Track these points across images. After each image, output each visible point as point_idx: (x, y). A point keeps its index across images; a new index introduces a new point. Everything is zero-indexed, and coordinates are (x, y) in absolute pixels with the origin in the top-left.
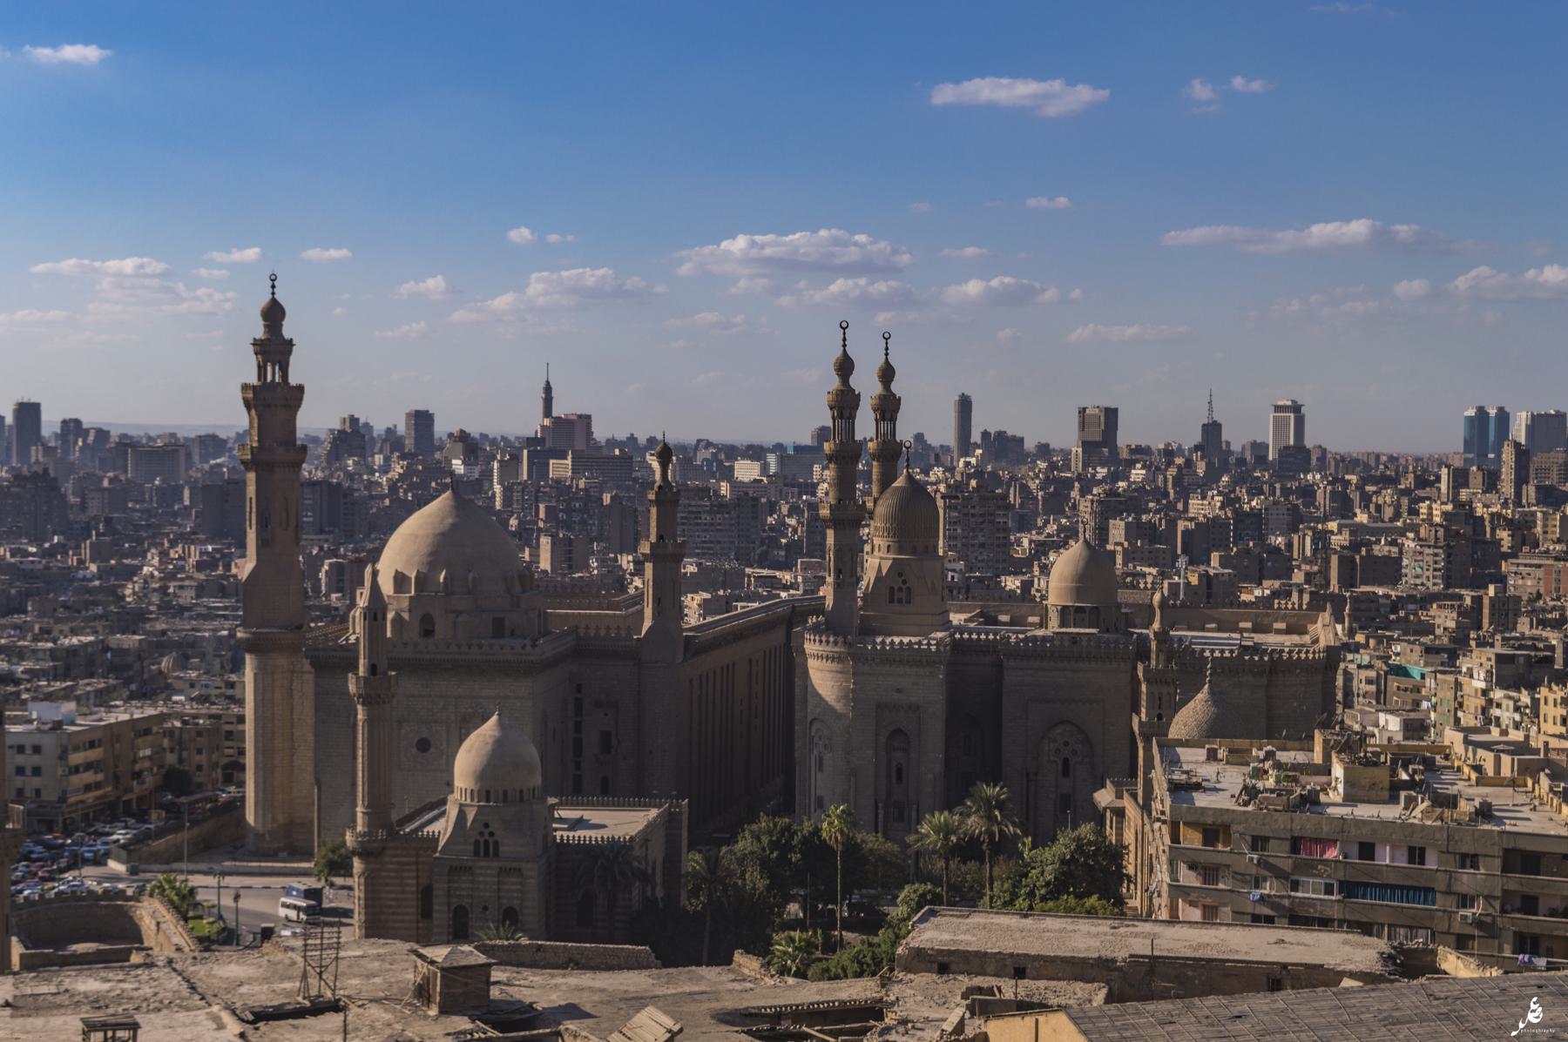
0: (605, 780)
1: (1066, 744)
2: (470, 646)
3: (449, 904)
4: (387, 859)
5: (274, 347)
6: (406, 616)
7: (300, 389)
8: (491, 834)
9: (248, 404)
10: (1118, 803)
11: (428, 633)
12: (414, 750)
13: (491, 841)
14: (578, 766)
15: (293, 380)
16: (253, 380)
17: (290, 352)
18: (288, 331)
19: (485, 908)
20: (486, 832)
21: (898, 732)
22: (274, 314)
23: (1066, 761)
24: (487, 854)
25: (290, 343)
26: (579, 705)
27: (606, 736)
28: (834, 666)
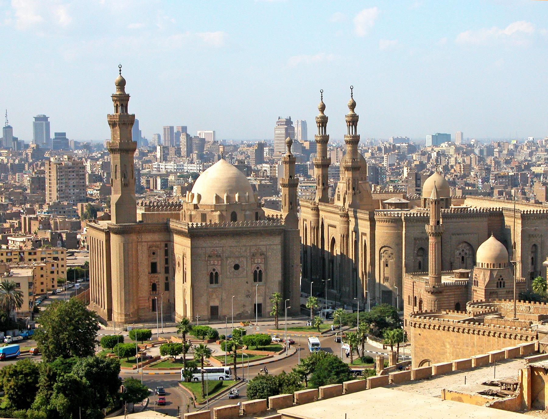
1: (463, 251)
4: (444, 294)
5: (122, 100)
6: (224, 213)
7: (133, 116)
8: (502, 279)
13: (502, 282)
15: (130, 112)
18: (127, 91)
22: (121, 84)
23: (463, 257)
24: (500, 287)
25: (128, 96)
28: (393, 224)
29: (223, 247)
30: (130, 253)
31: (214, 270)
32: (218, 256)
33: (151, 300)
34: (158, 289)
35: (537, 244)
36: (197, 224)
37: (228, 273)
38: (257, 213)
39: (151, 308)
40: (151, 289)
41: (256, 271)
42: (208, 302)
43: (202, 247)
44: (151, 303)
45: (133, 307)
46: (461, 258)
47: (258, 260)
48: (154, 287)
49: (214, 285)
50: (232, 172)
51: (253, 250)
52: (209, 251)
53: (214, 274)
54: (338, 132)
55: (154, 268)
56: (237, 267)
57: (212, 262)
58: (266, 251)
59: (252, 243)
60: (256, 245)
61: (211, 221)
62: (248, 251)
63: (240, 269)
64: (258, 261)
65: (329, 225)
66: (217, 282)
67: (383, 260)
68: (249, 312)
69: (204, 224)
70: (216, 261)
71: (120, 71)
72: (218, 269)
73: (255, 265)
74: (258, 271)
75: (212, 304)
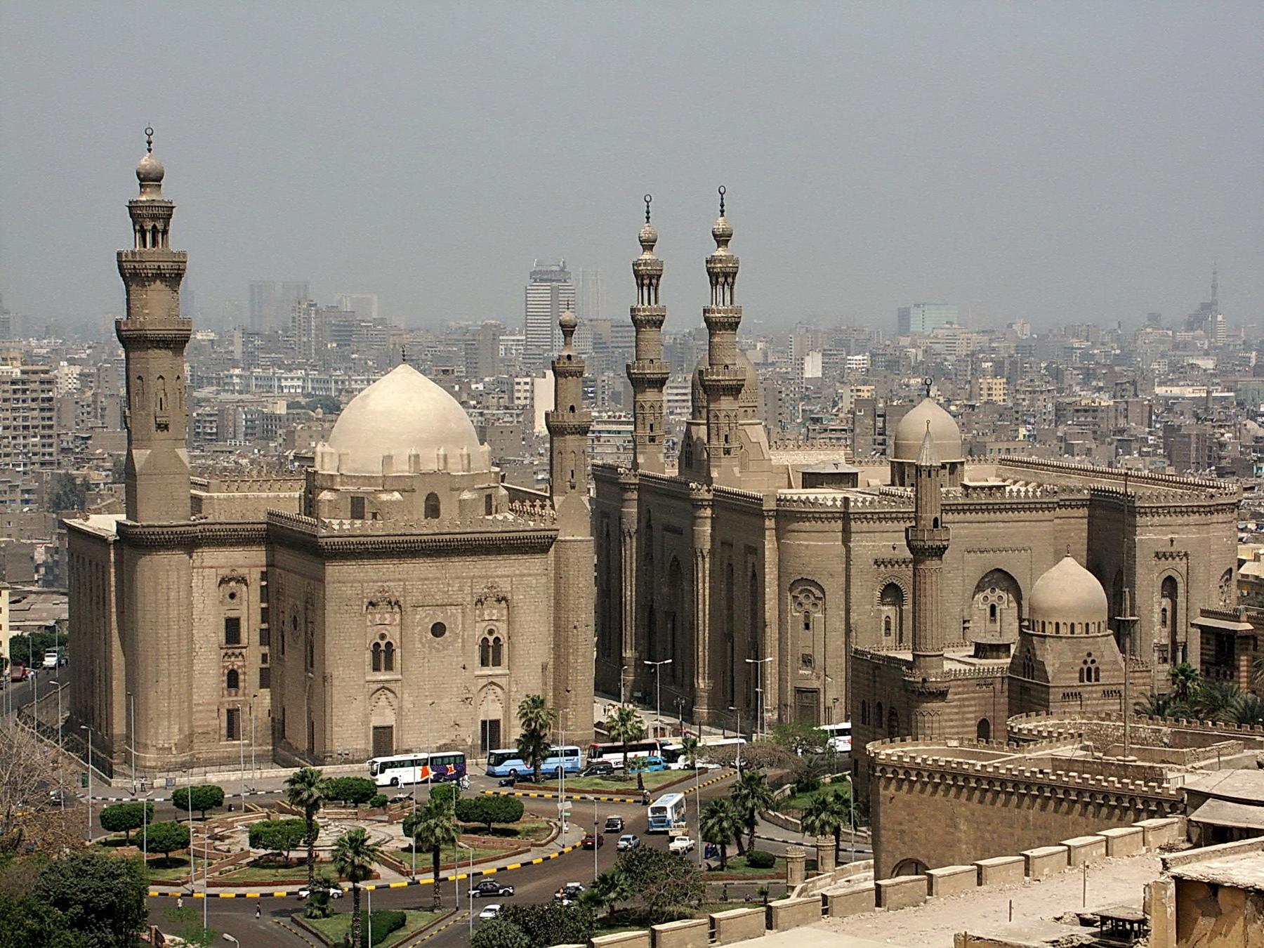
12: (430, 635)
13: (1093, 667)
20: (1089, 660)
23: (993, 608)
24: (1089, 679)
29: (404, 580)
30: (173, 594)
31: (383, 637)
32: (394, 604)
33: (224, 711)
34: (241, 684)
35: (1174, 575)
36: (341, 524)
37: (418, 645)
38: (489, 497)
39: (224, 732)
40: (225, 685)
41: (485, 640)
42: (367, 717)
43: (352, 582)
44: (225, 718)
45: (180, 730)
47: (494, 612)
48: (233, 679)
49: (382, 676)
51: (480, 589)
52: (371, 591)
53: (383, 648)
54: (685, 299)
55: (232, 628)
56: (438, 630)
57: (378, 616)
58: (511, 592)
59: (476, 572)
60: (487, 577)
61: (374, 516)
62: (467, 589)
63: (447, 634)
64: (491, 614)
65: (667, 528)
66: (389, 667)
68: (469, 741)
69: (358, 523)
70: (387, 616)
72: (394, 635)
73: (484, 624)
74: (491, 639)
75: (377, 721)
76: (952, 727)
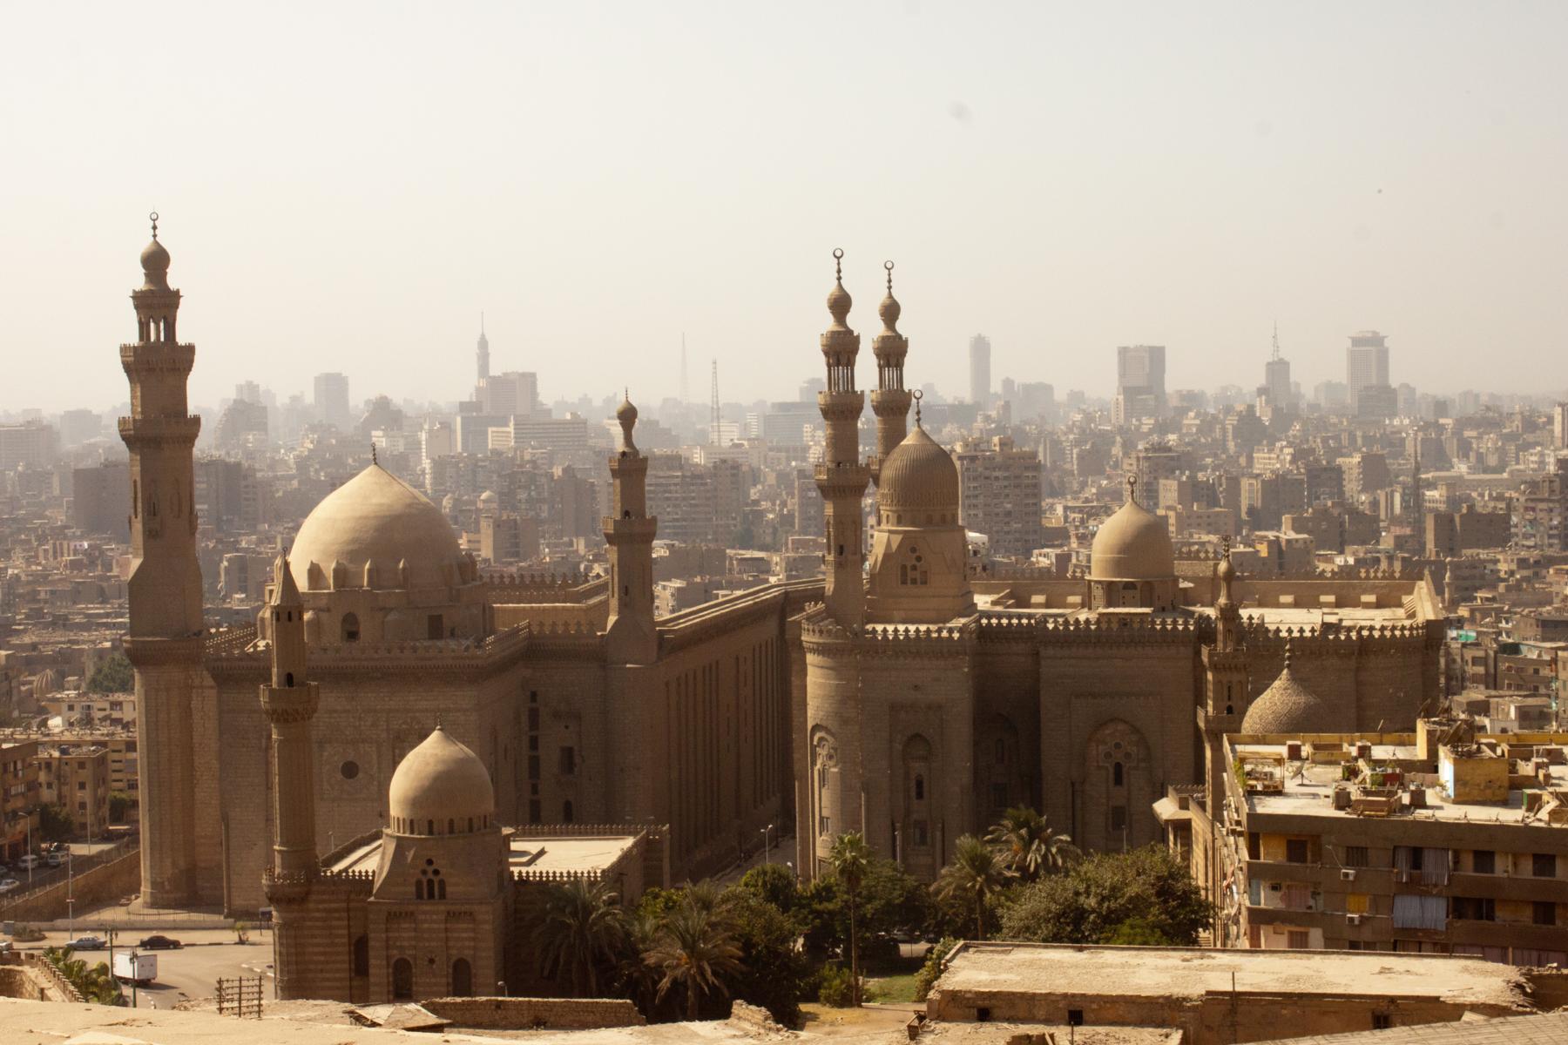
0: (568, 805)
1: (1118, 746)
2: (402, 650)
3: (388, 958)
4: (311, 906)
5: (157, 302)
7: (190, 349)
8: (436, 872)
9: (128, 368)
10: (1184, 815)
11: (352, 635)
12: (340, 776)
13: (436, 879)
14: (535, 790)
15: (182, 338)
16: (134, 340)
17: (177, 306)
18: (174, 279)
19: (432, 961)
20: (430, 869)
21: (917, 737)
22: (156, 262)
23: (1118, 767)
24: (431, 895)
25: (176, 295)
26: (534, 715)
27: (568, 753)
45: (174, 864)
46: (1111, 770)
50: (375, 501)
63: (360, 775)
67: (818, 766)
71: (155, 228)
76: (318, 945)
